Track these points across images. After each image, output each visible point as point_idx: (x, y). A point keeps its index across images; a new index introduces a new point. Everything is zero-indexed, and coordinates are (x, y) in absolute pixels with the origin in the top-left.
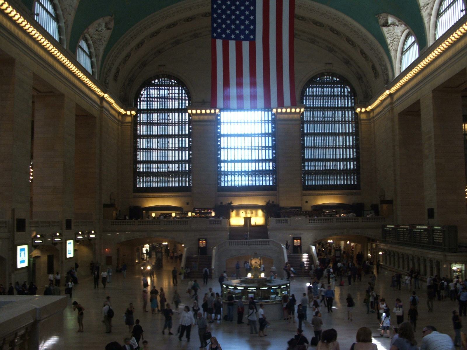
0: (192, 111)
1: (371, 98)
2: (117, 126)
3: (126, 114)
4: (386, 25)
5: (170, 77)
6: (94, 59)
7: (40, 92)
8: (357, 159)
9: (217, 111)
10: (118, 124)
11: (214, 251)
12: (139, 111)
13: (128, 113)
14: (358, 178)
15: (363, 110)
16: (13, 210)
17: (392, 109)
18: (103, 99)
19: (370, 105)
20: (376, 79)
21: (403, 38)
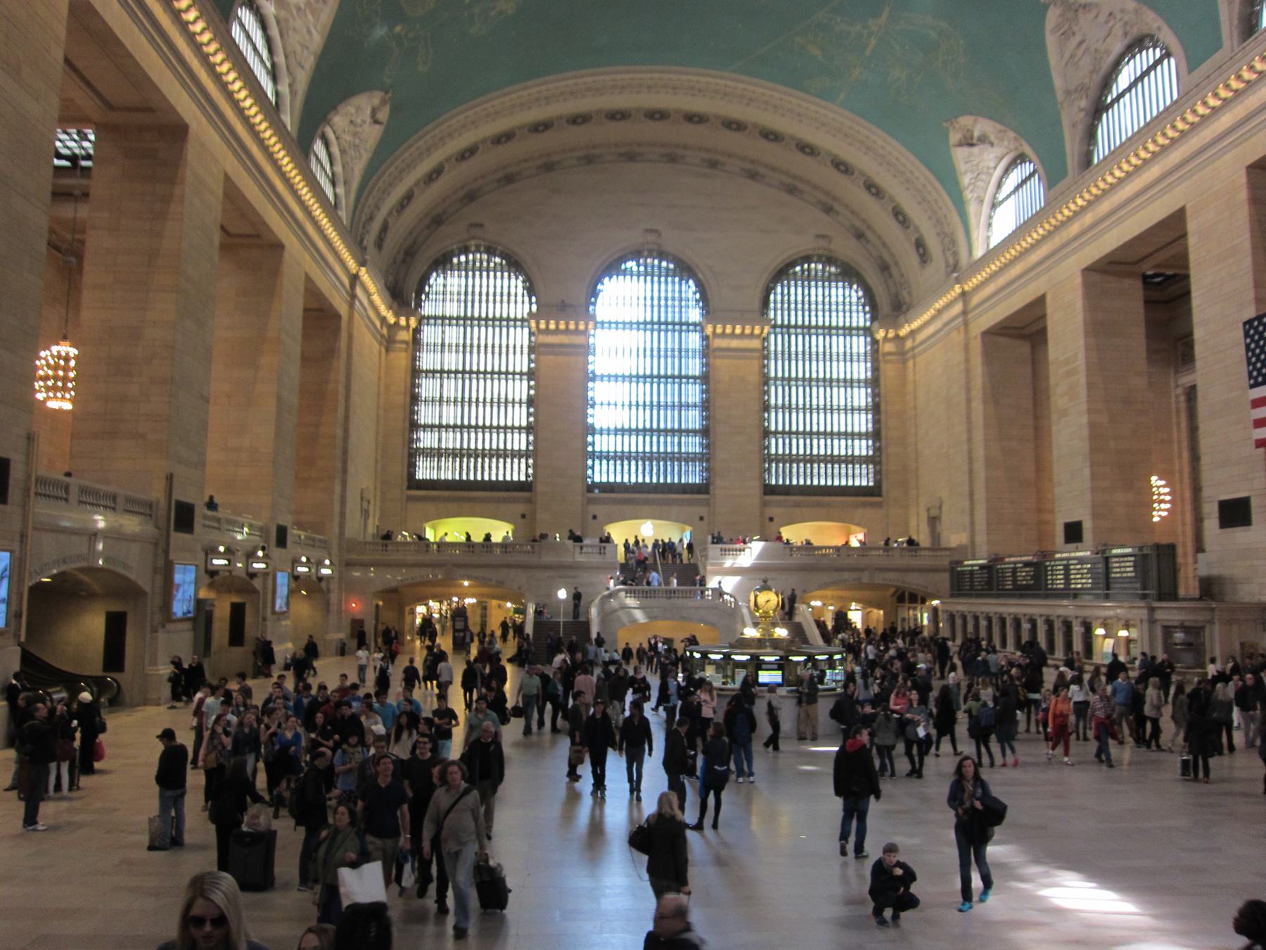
1: (908, 309)
2: (376, 345)
3: (397, 324)
4: (968, 142)
5: (491, 251)
8: (876, 435)
9: (591, 325)
11: (594, 612)
12: (422, 320)
13: (403, 321)
14: (877, 473)
15: (891, 334)
16: (170, 478)
17: (966, 324)
18: (355, 278)
19: (909, 322)
20: (923, 267)
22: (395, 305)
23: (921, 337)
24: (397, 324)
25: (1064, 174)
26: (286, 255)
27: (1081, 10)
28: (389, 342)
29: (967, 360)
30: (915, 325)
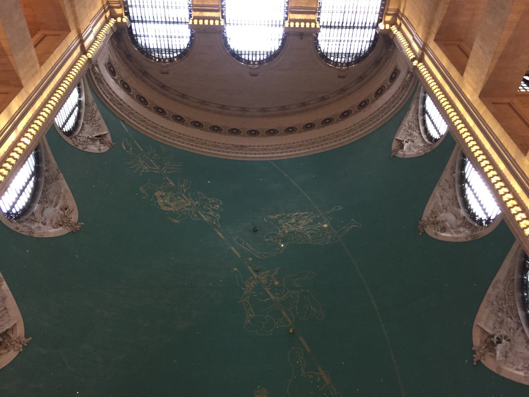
0: (316, 26)
2: (406, 14)
6: (420, 107)
7: (509, 104)
9: (287, 25)
10: (402, 16)
12: (376, 27)
13: (388, 26)
15: (119, 19)
17: (80, 35)
18: (421, 60)
21: (82, 121)
22: (391, 37)
23: (103, 19)
24: (391, 26)
25: (47, 135)
26: (479, 91)
27: (61, 223)
28: (397, 15)
29: (74, 13)
30: (107, 27)
